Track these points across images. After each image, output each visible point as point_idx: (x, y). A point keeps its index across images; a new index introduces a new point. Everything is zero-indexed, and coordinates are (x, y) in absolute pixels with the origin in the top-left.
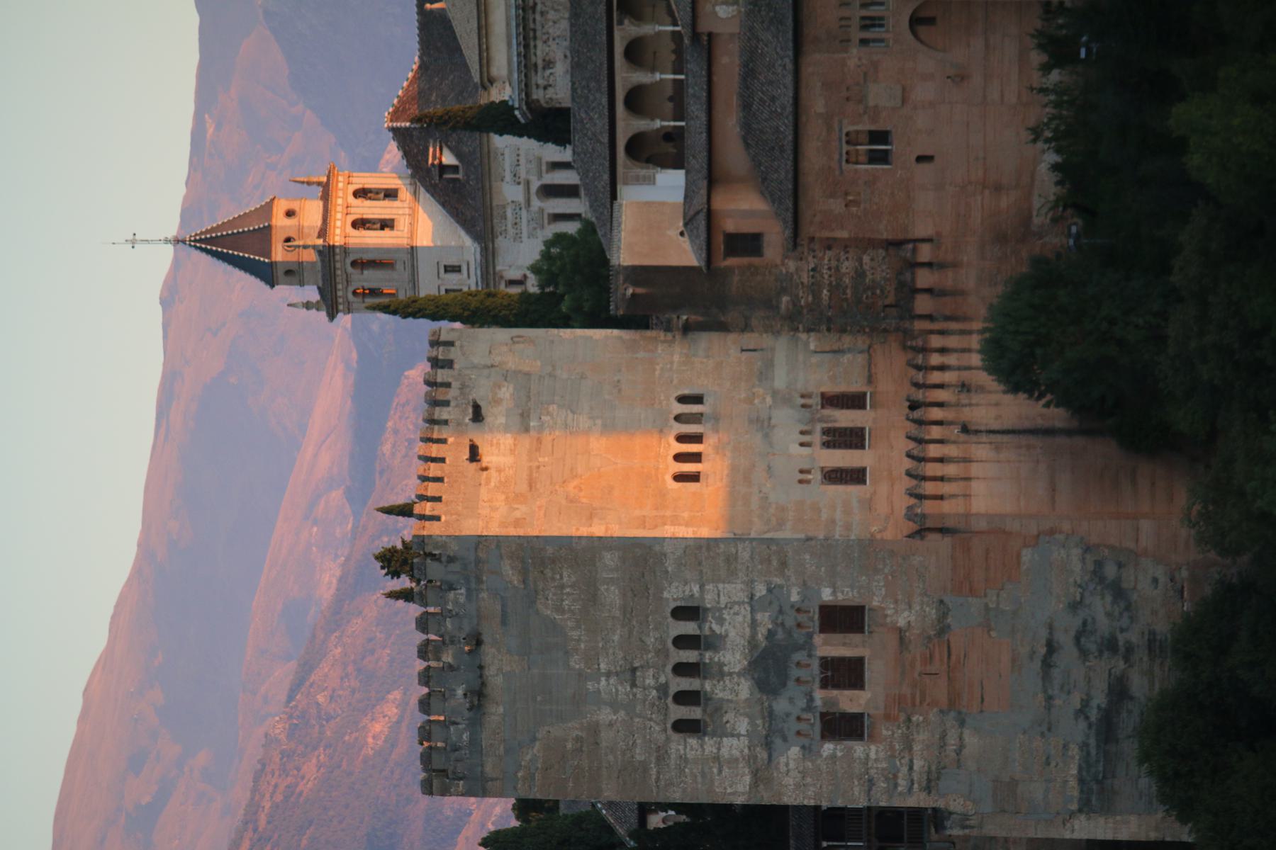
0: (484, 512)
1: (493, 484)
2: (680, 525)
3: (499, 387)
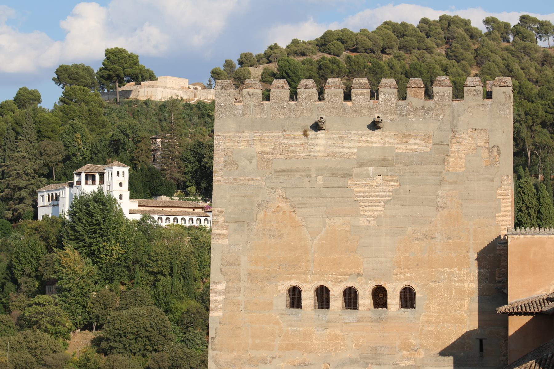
0: (247, 135)
1: (285, 141)
2: (227, 293)
3: (426, 140)
